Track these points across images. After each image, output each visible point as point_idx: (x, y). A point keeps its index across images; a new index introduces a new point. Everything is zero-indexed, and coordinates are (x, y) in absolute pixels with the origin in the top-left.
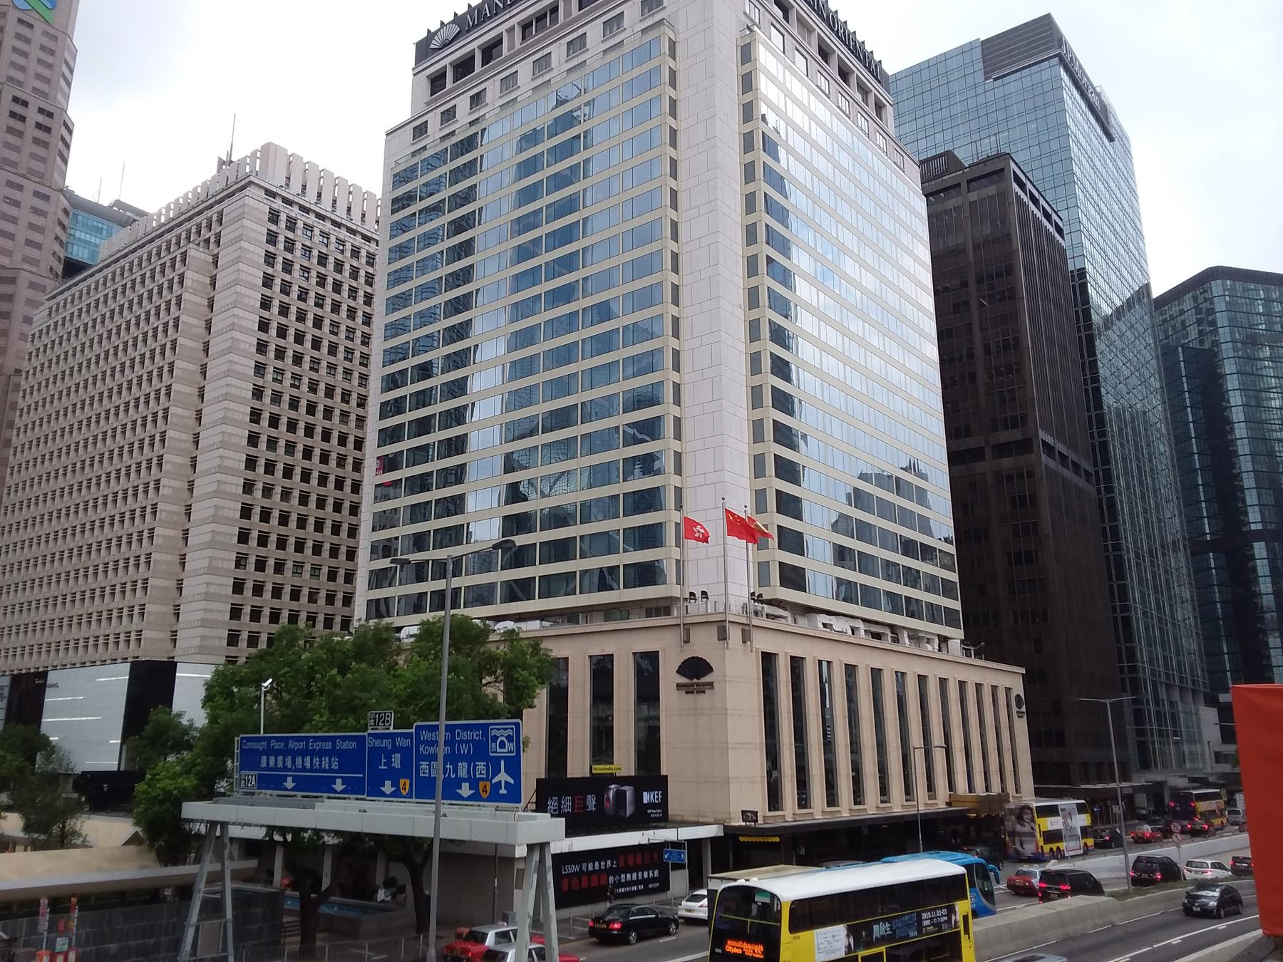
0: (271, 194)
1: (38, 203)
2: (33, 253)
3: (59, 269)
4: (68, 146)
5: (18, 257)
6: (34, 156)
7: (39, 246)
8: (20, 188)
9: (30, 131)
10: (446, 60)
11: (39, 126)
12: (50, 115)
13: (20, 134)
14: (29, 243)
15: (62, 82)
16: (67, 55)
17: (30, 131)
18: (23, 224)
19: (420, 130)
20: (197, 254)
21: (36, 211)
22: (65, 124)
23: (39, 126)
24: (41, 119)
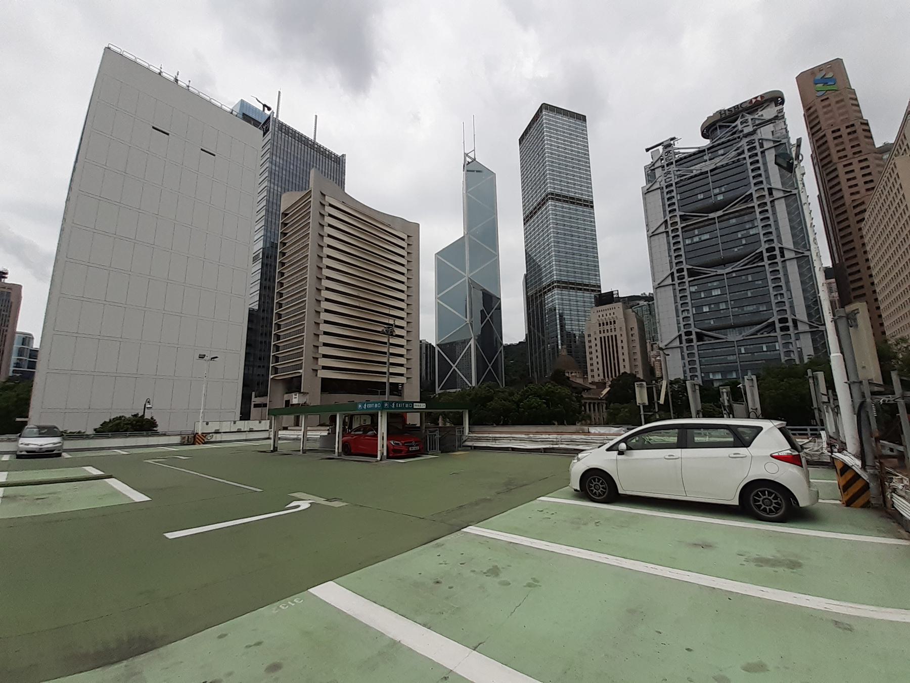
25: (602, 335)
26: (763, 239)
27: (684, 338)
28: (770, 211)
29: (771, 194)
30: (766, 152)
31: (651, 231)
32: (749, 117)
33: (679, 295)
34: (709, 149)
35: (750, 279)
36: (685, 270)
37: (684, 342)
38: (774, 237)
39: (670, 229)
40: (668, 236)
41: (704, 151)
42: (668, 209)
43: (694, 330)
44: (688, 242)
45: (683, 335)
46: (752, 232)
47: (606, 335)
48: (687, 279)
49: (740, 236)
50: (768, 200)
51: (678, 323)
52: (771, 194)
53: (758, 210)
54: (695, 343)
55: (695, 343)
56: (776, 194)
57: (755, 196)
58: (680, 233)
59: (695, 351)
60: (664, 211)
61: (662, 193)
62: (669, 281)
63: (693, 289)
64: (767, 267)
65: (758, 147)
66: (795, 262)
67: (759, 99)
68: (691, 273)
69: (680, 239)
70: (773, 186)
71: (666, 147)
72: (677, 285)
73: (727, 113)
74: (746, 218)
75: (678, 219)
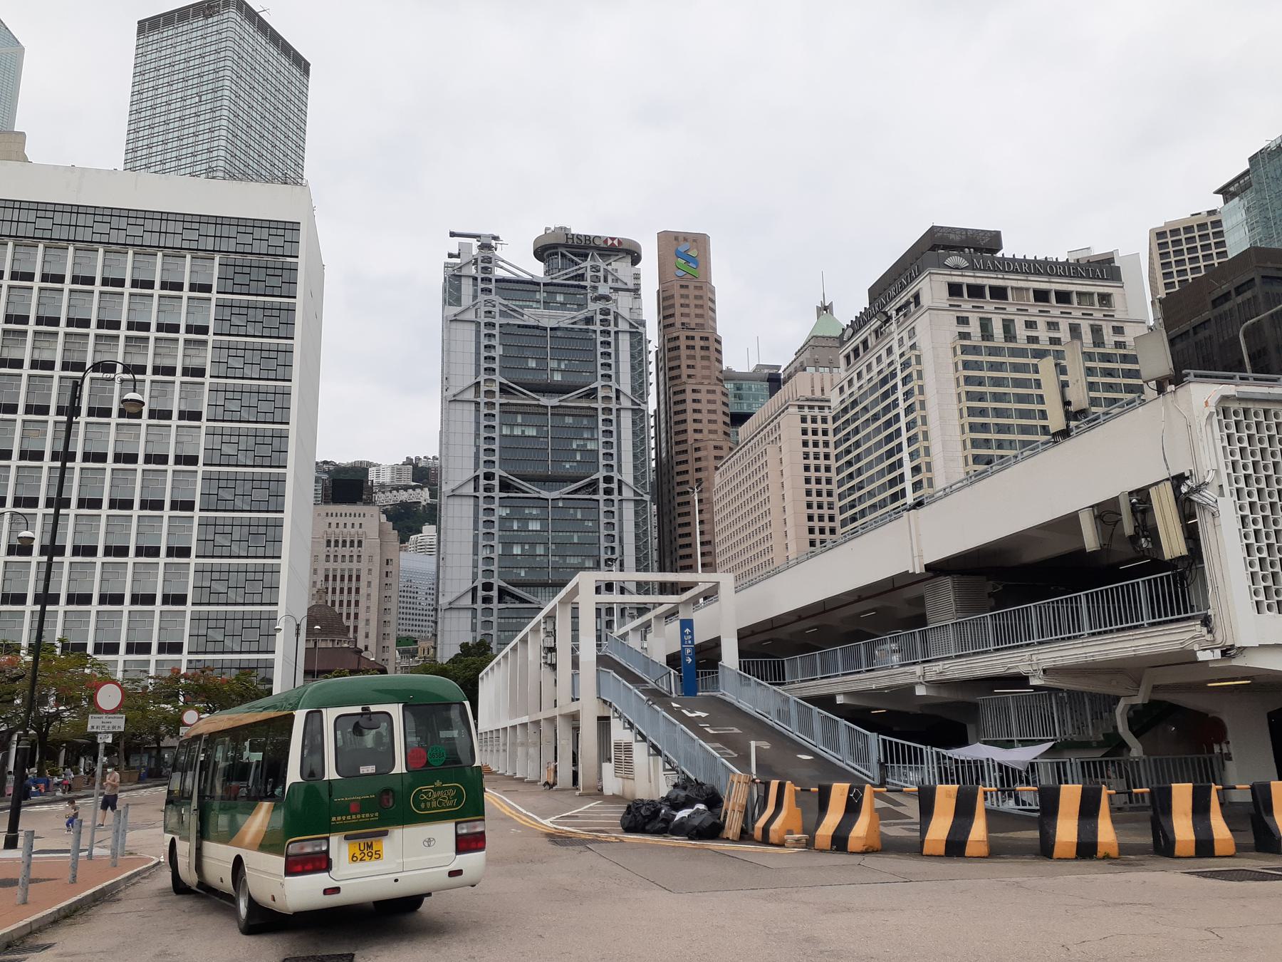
0: (801, 407)
1: (711, 397)
2: (713, 427)
3: (731, 430)
4: (719, 352)
6: (703, 368)
7: (715, 422)
9: (698, 353)
10: (849, 348)
12: (707, 339)
13: (693, 357)
14: (710, 421)
16: (710, 295)
19: (842, 390)
20: (772, 450)
21: (709, 402)
23: (702, 348)
24: (702, 343)
25: (331, 565)
26: (602, 462)
27: (481, 593)
29: (618, 398)
32: (601, 264)
33: (482, 518)
34: (545, 284)
35: (579, 516)
36: (497, 477)
37: (479, 600)
38: (614, 462)
39: (482, 399)
40: (477, 410)
41: (538, 284)
42: (484, 365)
43: (497, 582)
44: (506, 431)
45: (480, 588)
46: (591, 446)
47: (339, 565)
48: (497, 494)
49: (574, 447)
50: (613, 405)
51: (475, 566)
52: (618, 398)
53: (601, 417)
54: (495, 605)
55: (495, 605)
56: (625, 403)
57: (601, 394)
58: (496, 411)
59: (494, 619)
60: (478, 365)
61: (478, 332)
62: (469, 489)
63: (504, 512)
64: (601, 503)
66: (632, 505)
67: (616, 242)
68: (505, 486)
69: (496, 423)
70: (622, 388)
71: (482, 247)
72: (481, 500)
74: (585, 422)
75: (496, 388)
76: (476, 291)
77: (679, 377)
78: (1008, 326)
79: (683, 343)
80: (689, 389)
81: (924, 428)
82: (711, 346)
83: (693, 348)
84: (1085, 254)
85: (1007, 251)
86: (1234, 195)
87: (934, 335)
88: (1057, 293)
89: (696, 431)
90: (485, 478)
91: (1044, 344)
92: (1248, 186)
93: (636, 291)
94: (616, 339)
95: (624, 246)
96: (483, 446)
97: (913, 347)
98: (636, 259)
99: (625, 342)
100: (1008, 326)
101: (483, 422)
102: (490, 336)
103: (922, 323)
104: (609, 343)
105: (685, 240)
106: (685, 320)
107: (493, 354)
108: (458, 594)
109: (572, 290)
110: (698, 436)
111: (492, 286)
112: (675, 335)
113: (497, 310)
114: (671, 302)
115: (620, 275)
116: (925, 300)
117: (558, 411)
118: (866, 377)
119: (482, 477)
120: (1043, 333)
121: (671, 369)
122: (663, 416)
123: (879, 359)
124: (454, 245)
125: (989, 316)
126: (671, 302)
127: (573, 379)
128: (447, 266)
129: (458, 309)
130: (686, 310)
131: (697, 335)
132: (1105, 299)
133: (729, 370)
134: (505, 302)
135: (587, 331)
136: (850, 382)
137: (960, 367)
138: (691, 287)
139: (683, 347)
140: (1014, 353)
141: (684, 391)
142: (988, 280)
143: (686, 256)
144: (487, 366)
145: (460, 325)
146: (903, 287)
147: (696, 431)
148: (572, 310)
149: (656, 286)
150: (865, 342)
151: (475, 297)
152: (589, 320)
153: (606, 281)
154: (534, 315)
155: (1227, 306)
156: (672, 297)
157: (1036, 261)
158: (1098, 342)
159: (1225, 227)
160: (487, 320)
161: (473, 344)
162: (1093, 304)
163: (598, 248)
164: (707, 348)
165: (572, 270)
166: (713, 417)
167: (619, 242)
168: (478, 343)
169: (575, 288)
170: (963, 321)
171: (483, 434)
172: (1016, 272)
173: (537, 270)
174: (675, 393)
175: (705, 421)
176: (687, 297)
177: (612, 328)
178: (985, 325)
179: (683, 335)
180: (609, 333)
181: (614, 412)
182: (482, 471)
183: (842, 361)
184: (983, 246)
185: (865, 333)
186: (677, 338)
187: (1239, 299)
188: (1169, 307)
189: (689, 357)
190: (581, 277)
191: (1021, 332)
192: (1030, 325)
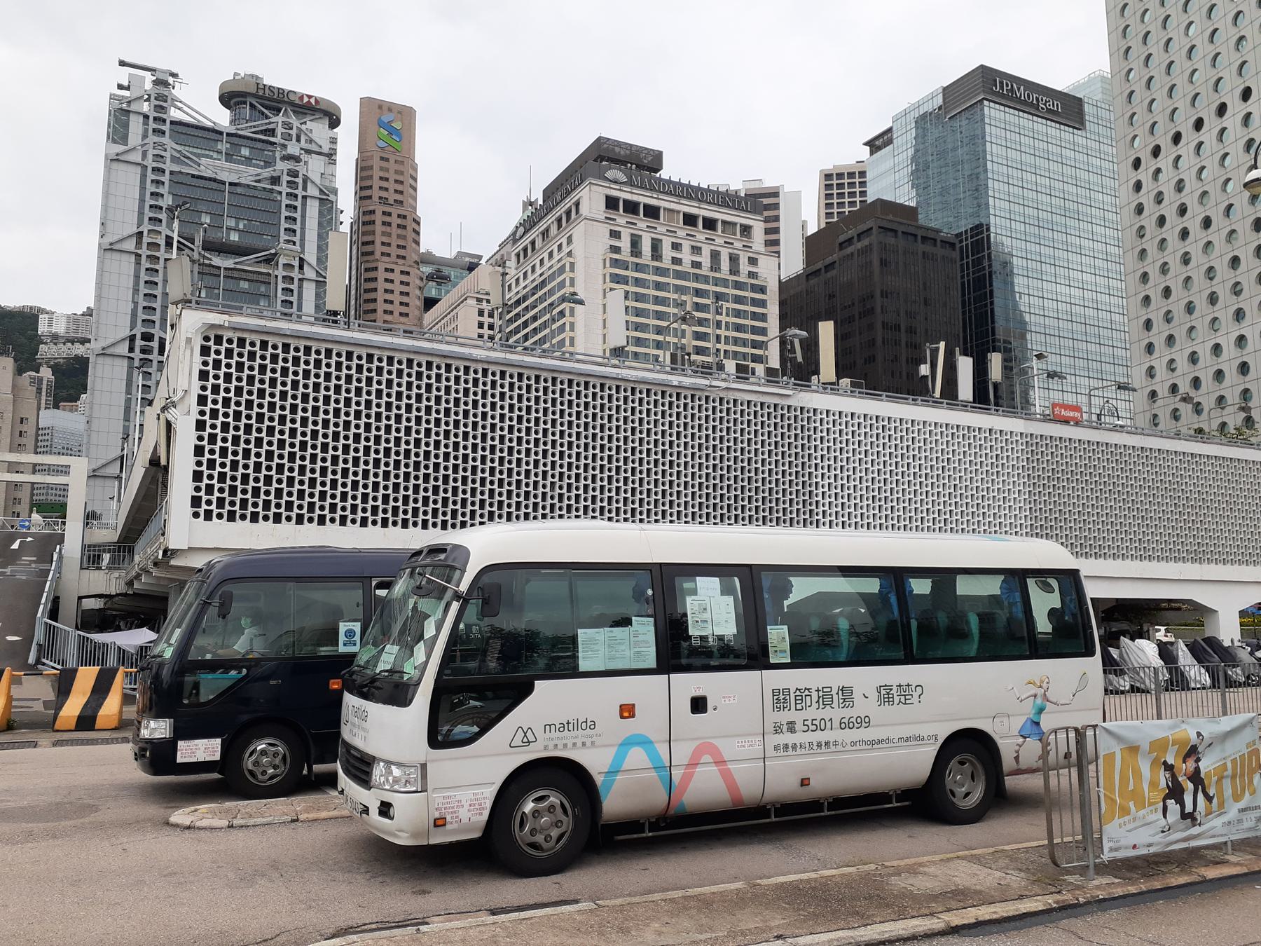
0: (479, 300)
1: (404, 278)
4: (418, 233)
5: (396, 314)
8: (392, 271)
9: (395, 231)
11: (399, 226)
12: (405, 217)
13: (389, 235)
14: (401, 304)
15: (411, 191)
16: (411, 171)
17: (395, 231)
18: (397, 293)
22: (414, 220)
23: (399, 226)
24: (399, 221)
28: (295, 293)
29: (301, 267)
30: (308, 200)
31: (110, 239)
34: (228, 134)
39: (144, 252)
40: (138, 263)
41: (221, 133)
42: (148, 213)
50: (296, 274)
52: (301, 267)
53: (281, 285)
56: (309, 273)
60: (141, 213)
61: (144, 176)
62: (123, 349)
65: (300, 186)
70: (306, 257)
71: (158, 82)
73: (267, 91)
74: (263, 289)
76: (146, 131)
77: (372, 253)
78: (656, 246)
79: (379, 218)
80: (381, 267)
81: (571, 334)
82: (410, 226)
83: (389, 224)
84: (757, 185)
85: (668, 172)
86: (879, 148)
87: (589, 244)
88: (705, 219)
89: (385, 312)
90: (142, 339)
91: (686, 267)
92: (890, 142)
93: (331, 156)
94: (304, 205)
95: (322, 106)
96: (142, 303)
97: (570, 254)
98: (334, 122)
99: (313, 208)
100: (656, 246)
101: (144, 277)
102: (158, 183)
103: (578, 231)
104: (295, 208)
105: (390, 110)
106: (384, 194)
107: (160, 203)
108: (104, 462)
109: (259, 145)
110: (388, 317)
111: (166, 128)
112: (371, 208)
113: (167, 155)
114: (369, 173)
115: (314, 136)
116: (584, 209)
117: (231, 274)
118: (530, 278)
119: (138, 336)
120: (686, 256)
121: (363, 244)
122: (353, 292)
123: (542, 261)
124: (124, 75)
125: (640, 233)
126: (369, 173)
127: (250, 241)
128: (113, 97)
129: (122, 148)
130: (384, 184)
131: (395, 211)
132: (746, 230)
133: (429, 253)
134: (178, 148)
135: (271, 191)
136: (517, 280)
137: (608, 279)
138: (392, 161)
139: (378, 222)
140: (658, 271)
141: (376, 269)
142: (643, 198)
143: (389, 128)
144: (152, 215)
145: (122, 166)
146: (568, 193)
147: (385, 312)
148: (258, 166)
149: (355, 154)
150: (533, 243)
151: (145, 136)
152: (275, 180)
153: (298, 140)
154: (214, 166)
155: (850, 250)
156: (371, 168)
157: (689, 186)
158: (734, 271)
159: (869, 176)
160: (155, 165)
161: (138, 189)
162: (734, 234)
163: (292, 104)
164: (405, 227)
165: (261, 123)
166: (405, 299)
167: (317, 101)
168: (143, 188)
169: (263, 145)
170: (615, 235)
171: (143, 290)
172: (670, 194)
173: (221, 117)
174: (366, 270)
175: (397, 303)
176: (387, 170)
177: (300, 192)
178: (635, 242)
179: (379, 209)
180: (296, 196)
181: (296, 281)
182: (138, 331)
183: (514, 258)
184: (643, 164)
185: (535, 233)
186: (373, 212)
187: (859, 245)
188: (813, 244)
189: (384, 234)
190: (272, 132)
191: (667, 252)
192: (676, 246)
